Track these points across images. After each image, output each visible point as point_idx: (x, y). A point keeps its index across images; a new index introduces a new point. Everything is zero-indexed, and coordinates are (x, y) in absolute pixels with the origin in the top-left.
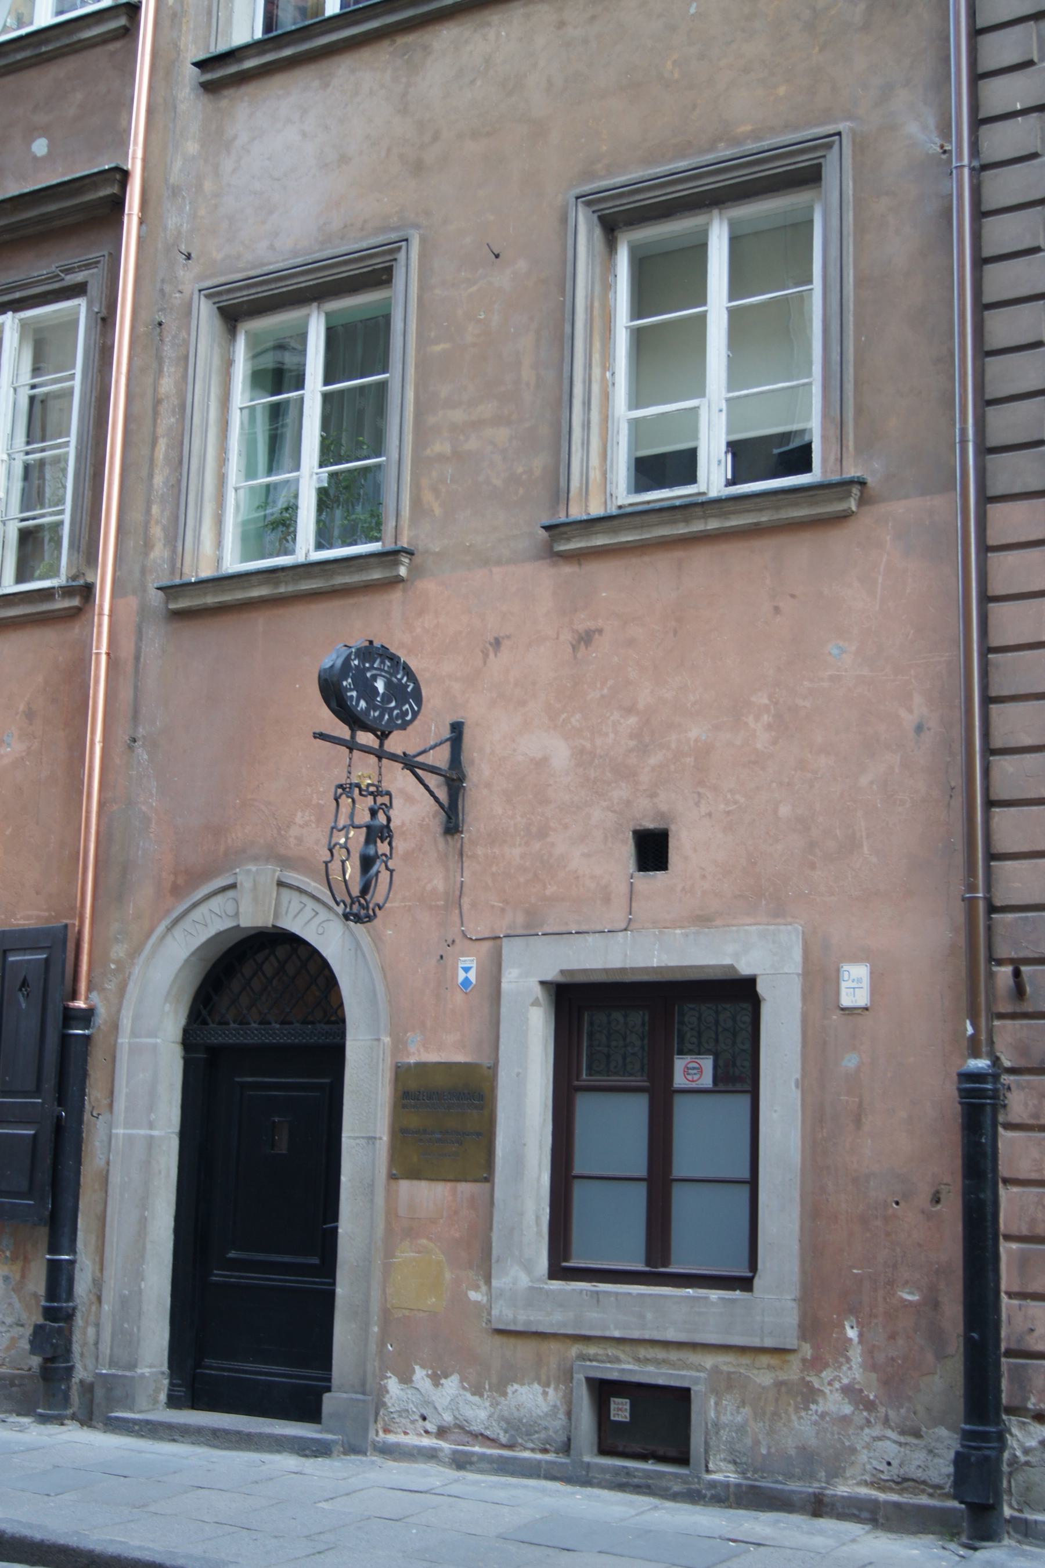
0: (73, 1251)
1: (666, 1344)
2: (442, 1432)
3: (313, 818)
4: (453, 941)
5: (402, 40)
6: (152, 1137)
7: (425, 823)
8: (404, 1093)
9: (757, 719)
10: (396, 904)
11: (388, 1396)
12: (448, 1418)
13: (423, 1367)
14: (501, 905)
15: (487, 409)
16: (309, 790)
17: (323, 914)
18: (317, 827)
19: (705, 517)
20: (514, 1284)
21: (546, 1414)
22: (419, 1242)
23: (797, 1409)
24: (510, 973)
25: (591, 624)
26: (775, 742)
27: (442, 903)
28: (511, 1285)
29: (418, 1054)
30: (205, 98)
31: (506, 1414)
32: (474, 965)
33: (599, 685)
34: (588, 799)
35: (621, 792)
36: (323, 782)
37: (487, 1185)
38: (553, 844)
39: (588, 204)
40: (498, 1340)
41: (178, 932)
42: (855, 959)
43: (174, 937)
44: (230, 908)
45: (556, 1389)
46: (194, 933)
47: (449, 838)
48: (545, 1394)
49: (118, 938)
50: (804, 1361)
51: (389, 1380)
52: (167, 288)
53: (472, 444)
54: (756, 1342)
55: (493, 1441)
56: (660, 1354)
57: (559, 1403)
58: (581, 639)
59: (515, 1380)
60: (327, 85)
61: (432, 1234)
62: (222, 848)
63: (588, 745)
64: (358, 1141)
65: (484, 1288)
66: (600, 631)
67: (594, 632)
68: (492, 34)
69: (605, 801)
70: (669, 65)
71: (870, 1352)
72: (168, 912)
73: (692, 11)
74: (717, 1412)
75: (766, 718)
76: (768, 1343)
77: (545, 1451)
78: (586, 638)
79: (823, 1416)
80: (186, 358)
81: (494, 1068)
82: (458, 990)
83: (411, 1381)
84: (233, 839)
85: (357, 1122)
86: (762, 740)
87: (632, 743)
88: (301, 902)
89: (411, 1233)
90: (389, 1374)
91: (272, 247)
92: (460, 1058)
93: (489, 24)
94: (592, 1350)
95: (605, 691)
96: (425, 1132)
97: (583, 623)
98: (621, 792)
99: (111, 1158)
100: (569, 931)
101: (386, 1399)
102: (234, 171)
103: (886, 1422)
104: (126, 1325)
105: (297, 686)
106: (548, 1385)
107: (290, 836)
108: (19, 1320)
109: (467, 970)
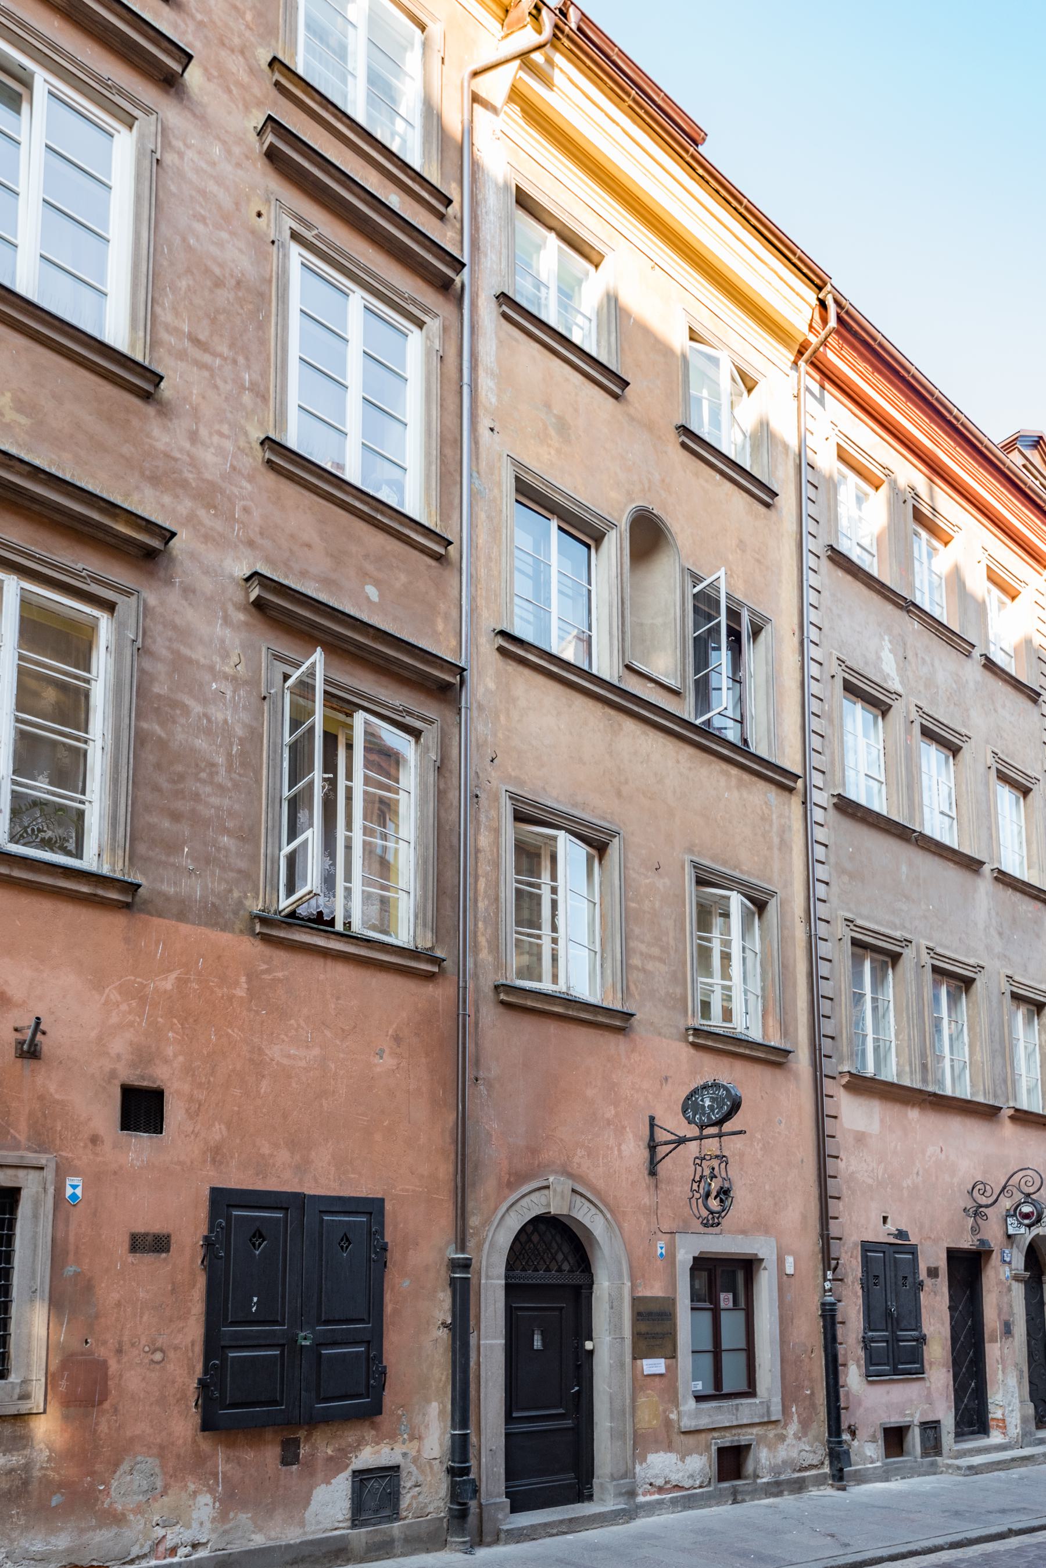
2: (660, 1490)
17: (593, 1210)
44: (544, 1201)
56: (739, 1431)
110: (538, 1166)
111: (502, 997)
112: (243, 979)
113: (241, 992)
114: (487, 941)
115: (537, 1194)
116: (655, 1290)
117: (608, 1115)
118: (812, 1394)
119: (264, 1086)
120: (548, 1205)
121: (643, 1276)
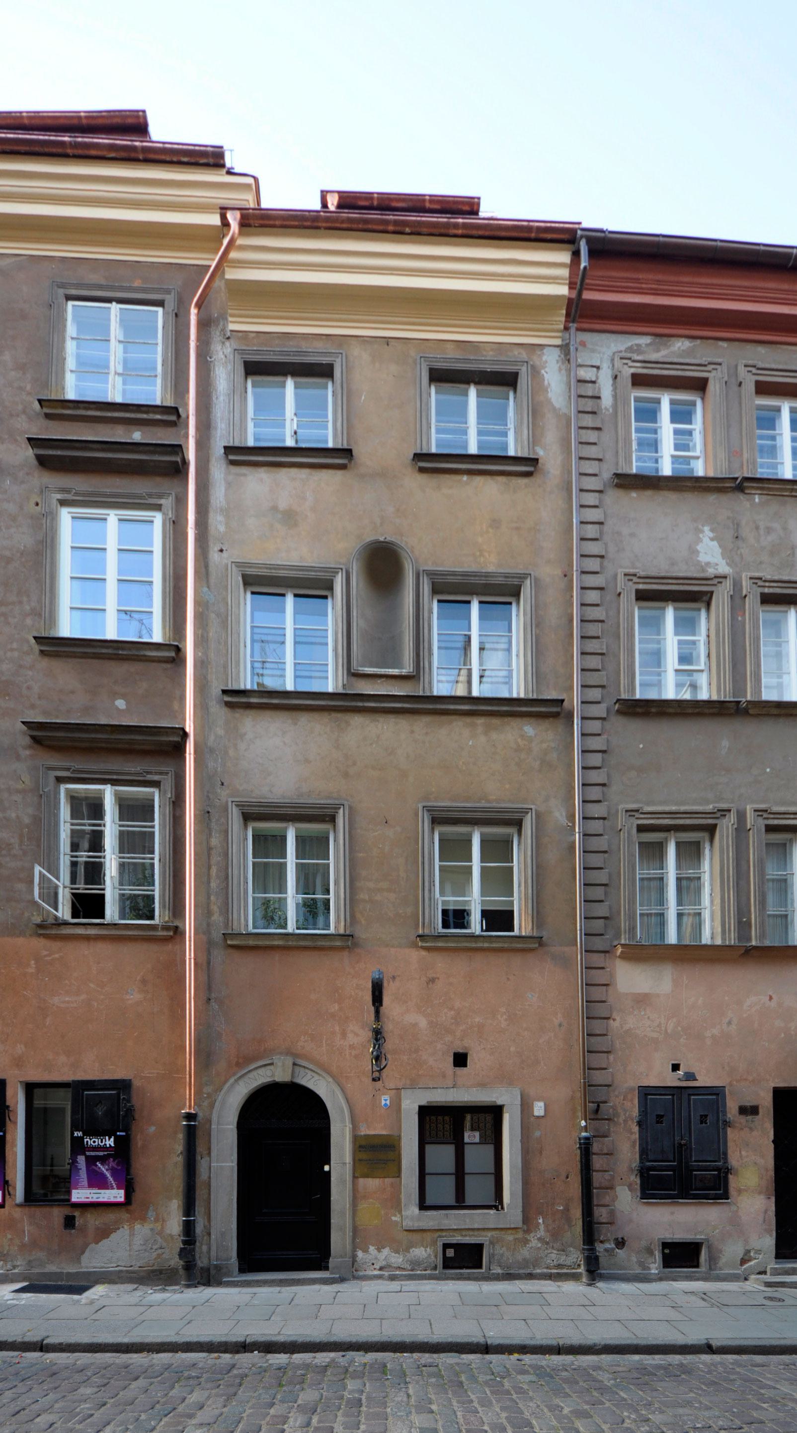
1: (473, 1230)
2: (381, 1269)
5: (334, 715)
9: (502, 1017)
12: (384, 1263)
13: (373, 1246)
15: (385, 885)
19: (483, 942)
23: (522, 1247)
25: (434, 976)
26: (508, 1025)
29: (364, 1131)
30: (225, 711)
35: (448, 1038)
37: (398, 1179)
39: (428, 811)
41: (241, 1083)
42: (539, 1100)
44: (269, 1073)
45: (430, 1248)
48: (426, 1251)
50: (524, 1231)
52: (211, 796)
53: (378, 897)
54: (508, 1226)
55: (404, 1269)
56: (471, 1233)
59: (412, 1247)
60: (296, 724)
62: (263, 1048)
65: (398, 1216)
66: (438, 978)
68: (380, 726)
70: (461, 763)
71: (546, 1226)
72: (234, 1074)
73: (470, 743)
74: (494, 1250)
75: (505, 1017)
76: (512, 1226)
77: (426, 1270)
78: (432, 980)
79: (531, 1248)
80: (227, 832)
81: (399, 1137)
86: (504, 1024)
87: (453, 1021)
91: (271, 791)
92: (384, 1133)
93: (378, 721)
94: (444, 1234)
96: (370, 1160)
97: (431, 974)
98: (448, 1038)
101: (357, 1259)
102: (246, 750)
103: (553, 1247)
109: (386, 1100)
111: (229, 942)
112: (33, 962)
113: (32, 970)
114: (218, 907)
115: (263, 1069)
116: (378, 1129)
118: (567, 1209)
119: (48, 1021)
120: (273, 1075)
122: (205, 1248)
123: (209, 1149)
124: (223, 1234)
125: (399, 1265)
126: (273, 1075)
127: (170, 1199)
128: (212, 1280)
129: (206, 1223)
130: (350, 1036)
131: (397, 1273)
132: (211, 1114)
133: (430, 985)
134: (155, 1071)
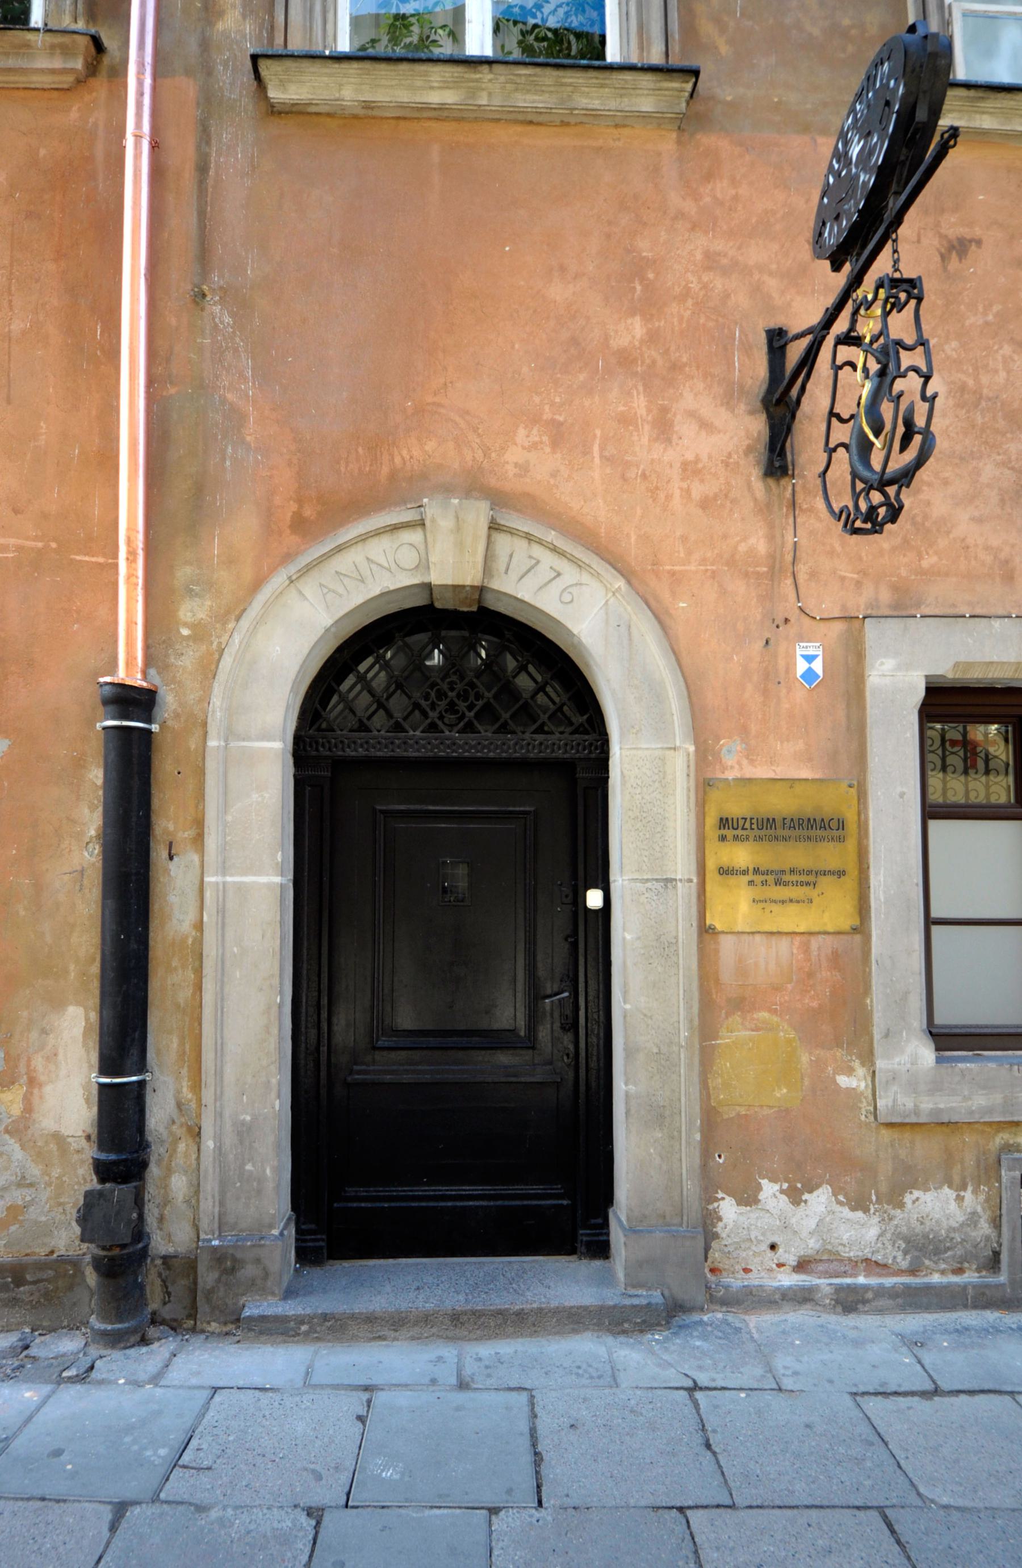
0: (142, 1067)
3: (545, 438)
4: (787, 620)
6: (224, 883)
7: (732, 460)
8: (721, 819)
10: (693, 568)
11: (720, 1224)
12: (813, 1244)
13: (772, 1180)
14: (855, 576)
16: (537, 399)
18: (554, 452)
20: (912, 1064)
21: (962, 1225)
22: (755, 1016)
24: (882, 664)
25: (964, 231)
27: (765, 569)
28: (909, 1066)
31: (904, 1229)
32: (820, 653)
33: (981, 308)
34: (975, 449)
36: (561, 390)
38: (928, 503)
40: (886, 1134)
41: (309, 587)
43: (300, 592)
44: (409, 558)
45: (975, 1192)
46: (341, 590)
47: (771, 482)
48: (960, 1199)
49: (193, 590)
51: (721, 1202)
57: (979, 1209)
58: (951, 248)
59: (913, 1185)
61: (776, 1004)
62: (385, 470)
63: (971, 382)
64: (649, 885)
65: (861, 1071)
66: (979, 242)
67: (970, 241)
69: (999, 454)
72: (287, 558)
77: (959, 1271)
82: (797, 684)
83: (757, 1201)
84: (403, 459)
85: (646, 859)
88: (530, 557)
89: (741, 1004)
90: (720, 1195)
95: (990, 318)
96: (756, 871)
99: (205, 918)
100: (960, 613)
101: (719, 1228)
104: (249, 1167)
105: (507, 249)
106: (964, 1188)
107: (507, 463)
108: (24, 1177)
109: (810, 659)
110: (393, 476)
117: (621, 341)
120: (424, 565)
121: (744, 730)
122: (179, 1184)
123: (199, 823)
124: (244, 1132)
125: (867, 1253)
126: (424, 565)
127: (58, 1004)
128: (202, 1306)
129: (187, 1094)
130: (685, 429)
131: (861, 1280)
132: (206, 698)
133: (954, 264)
134: (12, 541)
